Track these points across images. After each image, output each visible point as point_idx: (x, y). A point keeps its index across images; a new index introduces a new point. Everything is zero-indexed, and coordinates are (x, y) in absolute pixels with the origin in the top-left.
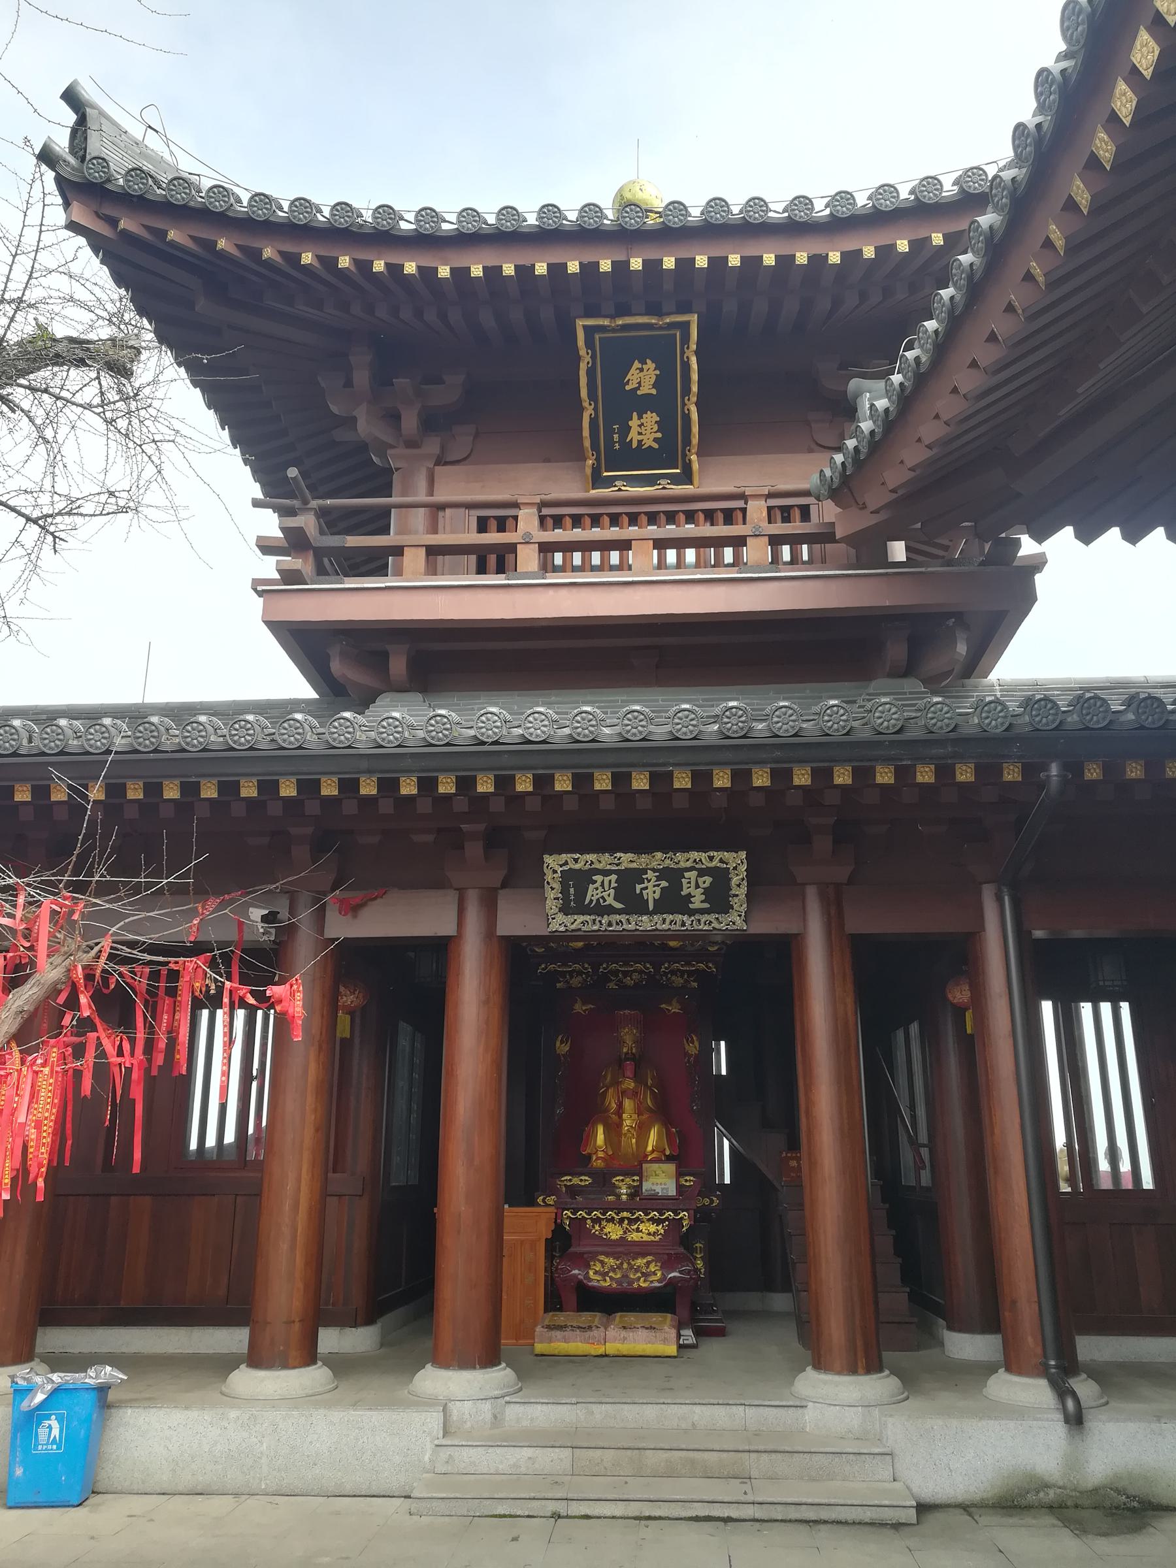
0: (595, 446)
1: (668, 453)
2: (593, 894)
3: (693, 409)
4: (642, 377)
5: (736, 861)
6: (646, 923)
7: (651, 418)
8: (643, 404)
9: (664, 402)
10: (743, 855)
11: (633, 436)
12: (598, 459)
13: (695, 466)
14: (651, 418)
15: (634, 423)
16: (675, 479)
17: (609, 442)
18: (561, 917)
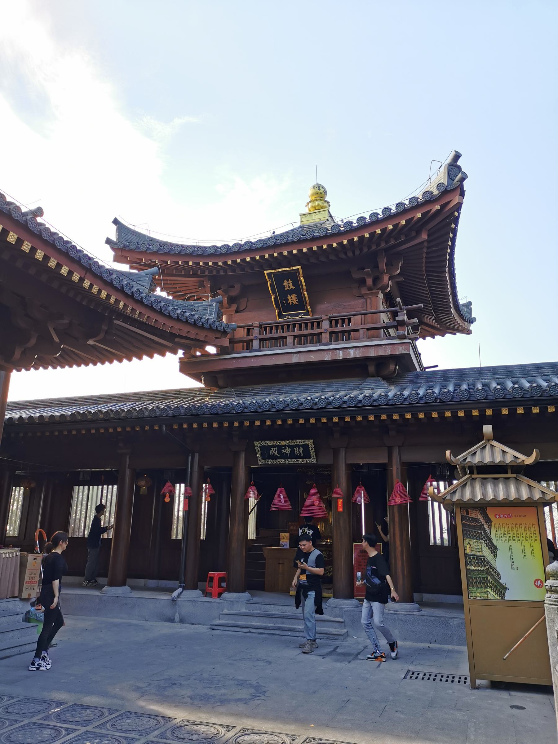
0: (277, 305)
1: (301, 305)
2: (272, 452)
3: (305, 293)
4: (288, 284)
5: (310, 442)
6: (287, 461)
7: (294, 296)
8: (291, 292)
9: (297, 291)
10: (312, 441)
11: (290, 301)
12: (280, 310)
13: (310, 310)
14: (294, 296)
15: (289, 297)
16: (305, 314)
17: (282, 303)
18: (263, 461)
